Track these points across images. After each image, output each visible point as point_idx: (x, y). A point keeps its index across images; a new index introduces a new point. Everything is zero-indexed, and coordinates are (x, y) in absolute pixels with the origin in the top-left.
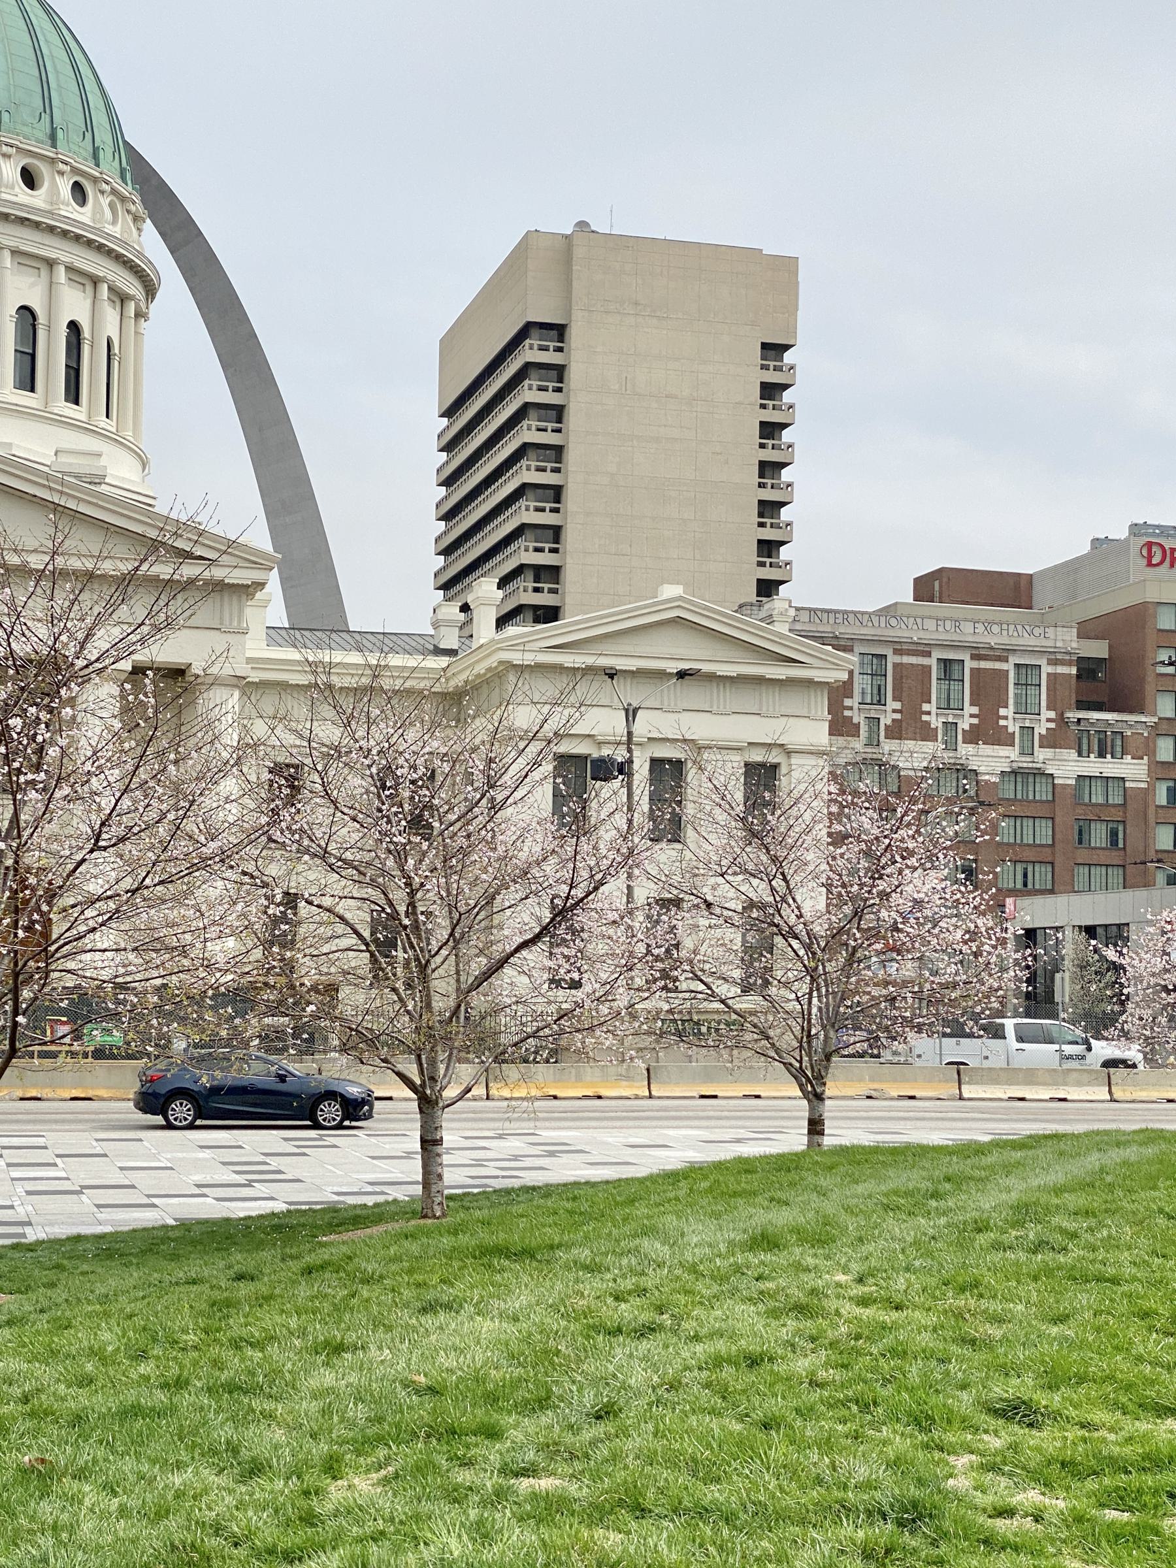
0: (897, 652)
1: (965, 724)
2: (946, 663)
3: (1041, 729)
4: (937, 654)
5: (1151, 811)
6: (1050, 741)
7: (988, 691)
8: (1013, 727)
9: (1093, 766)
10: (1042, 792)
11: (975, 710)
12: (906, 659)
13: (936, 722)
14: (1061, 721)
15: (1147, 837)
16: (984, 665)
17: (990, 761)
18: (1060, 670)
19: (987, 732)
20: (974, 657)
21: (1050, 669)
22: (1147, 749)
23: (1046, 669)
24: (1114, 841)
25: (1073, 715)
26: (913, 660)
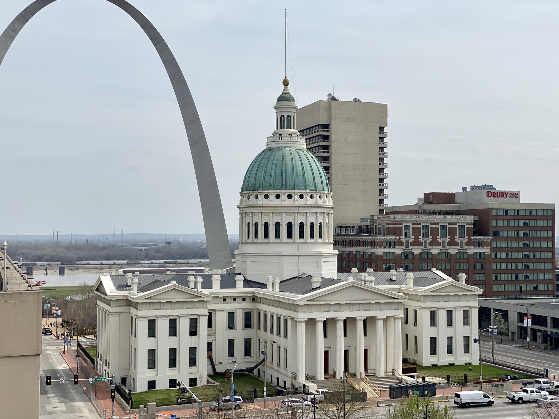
0: (431, 224)
1: (447, 241)
2: (442, 226)
3: (465, 241)
4: (440, 224)
5: (491, 260)
6: (468, 244)
7: (452, 232)
8: (459, 241)
9: (477, 249)
10: (466, 256)
11: (449, 237)
12: (433, 226)
13: (440, 241)
14: (470, 239)
15: (491, 266)
16: (451, 226)
17: (453, 250)
18: (469, 226)
19: (452, 243)
20: (449, 224)
21: (467, 226)
22: (489, 245)
23: (466, 226)
24: (482, 268)
25: (472, 237)
26: (435, 226)
